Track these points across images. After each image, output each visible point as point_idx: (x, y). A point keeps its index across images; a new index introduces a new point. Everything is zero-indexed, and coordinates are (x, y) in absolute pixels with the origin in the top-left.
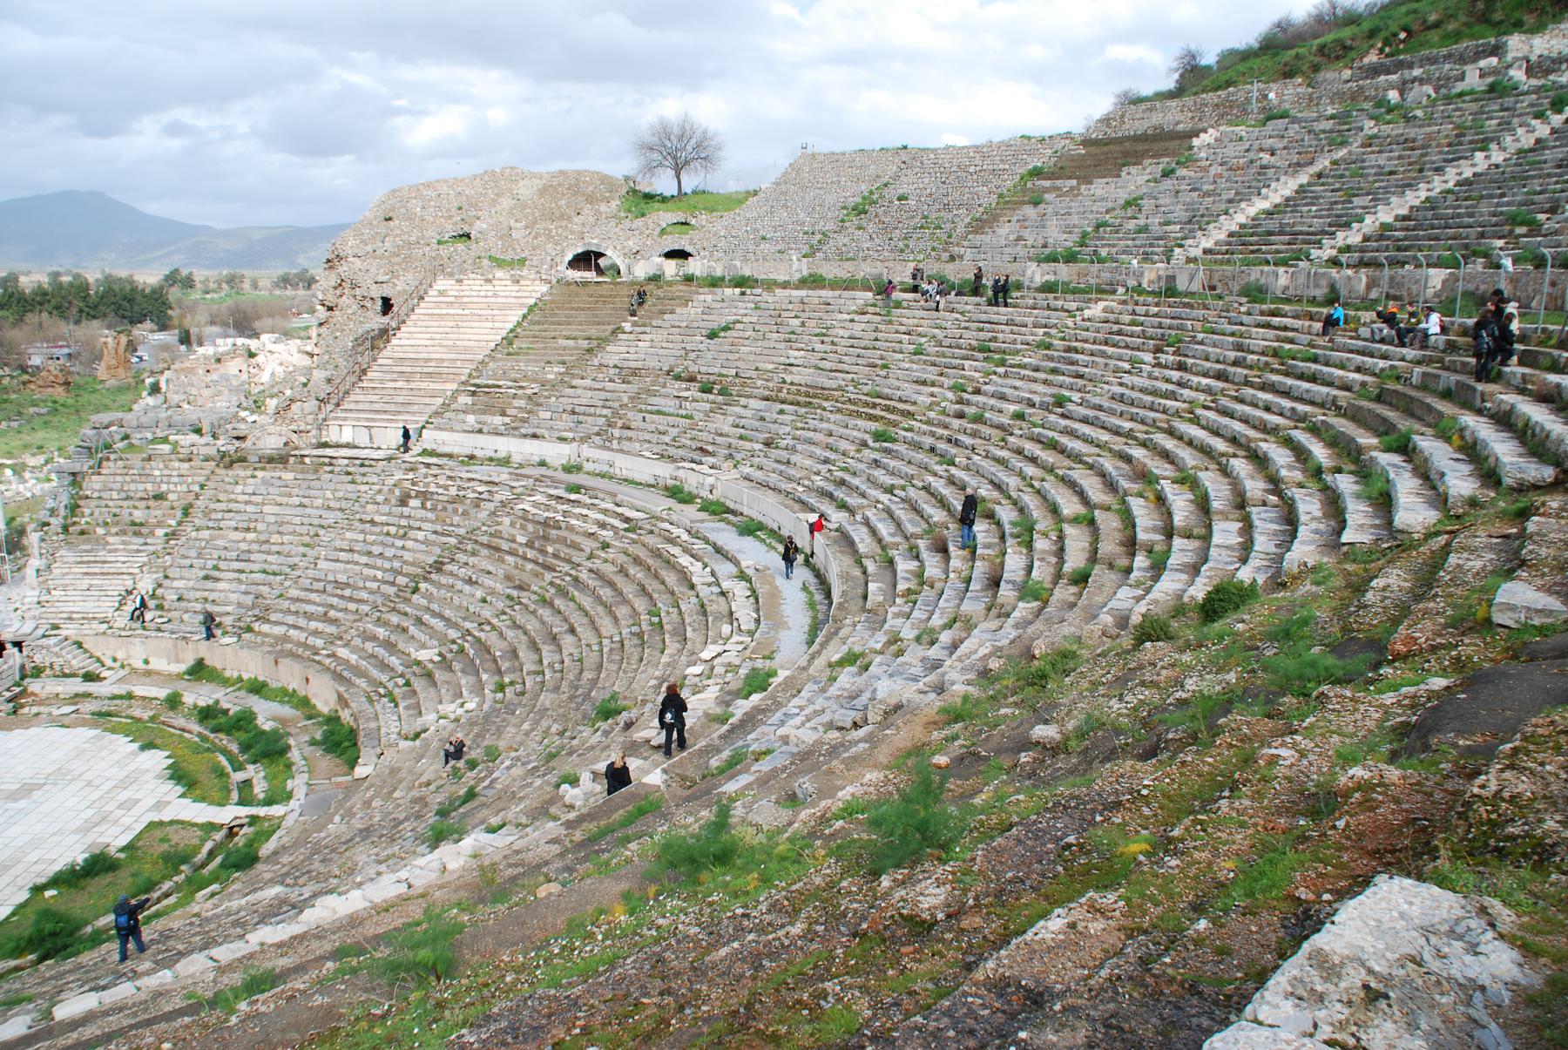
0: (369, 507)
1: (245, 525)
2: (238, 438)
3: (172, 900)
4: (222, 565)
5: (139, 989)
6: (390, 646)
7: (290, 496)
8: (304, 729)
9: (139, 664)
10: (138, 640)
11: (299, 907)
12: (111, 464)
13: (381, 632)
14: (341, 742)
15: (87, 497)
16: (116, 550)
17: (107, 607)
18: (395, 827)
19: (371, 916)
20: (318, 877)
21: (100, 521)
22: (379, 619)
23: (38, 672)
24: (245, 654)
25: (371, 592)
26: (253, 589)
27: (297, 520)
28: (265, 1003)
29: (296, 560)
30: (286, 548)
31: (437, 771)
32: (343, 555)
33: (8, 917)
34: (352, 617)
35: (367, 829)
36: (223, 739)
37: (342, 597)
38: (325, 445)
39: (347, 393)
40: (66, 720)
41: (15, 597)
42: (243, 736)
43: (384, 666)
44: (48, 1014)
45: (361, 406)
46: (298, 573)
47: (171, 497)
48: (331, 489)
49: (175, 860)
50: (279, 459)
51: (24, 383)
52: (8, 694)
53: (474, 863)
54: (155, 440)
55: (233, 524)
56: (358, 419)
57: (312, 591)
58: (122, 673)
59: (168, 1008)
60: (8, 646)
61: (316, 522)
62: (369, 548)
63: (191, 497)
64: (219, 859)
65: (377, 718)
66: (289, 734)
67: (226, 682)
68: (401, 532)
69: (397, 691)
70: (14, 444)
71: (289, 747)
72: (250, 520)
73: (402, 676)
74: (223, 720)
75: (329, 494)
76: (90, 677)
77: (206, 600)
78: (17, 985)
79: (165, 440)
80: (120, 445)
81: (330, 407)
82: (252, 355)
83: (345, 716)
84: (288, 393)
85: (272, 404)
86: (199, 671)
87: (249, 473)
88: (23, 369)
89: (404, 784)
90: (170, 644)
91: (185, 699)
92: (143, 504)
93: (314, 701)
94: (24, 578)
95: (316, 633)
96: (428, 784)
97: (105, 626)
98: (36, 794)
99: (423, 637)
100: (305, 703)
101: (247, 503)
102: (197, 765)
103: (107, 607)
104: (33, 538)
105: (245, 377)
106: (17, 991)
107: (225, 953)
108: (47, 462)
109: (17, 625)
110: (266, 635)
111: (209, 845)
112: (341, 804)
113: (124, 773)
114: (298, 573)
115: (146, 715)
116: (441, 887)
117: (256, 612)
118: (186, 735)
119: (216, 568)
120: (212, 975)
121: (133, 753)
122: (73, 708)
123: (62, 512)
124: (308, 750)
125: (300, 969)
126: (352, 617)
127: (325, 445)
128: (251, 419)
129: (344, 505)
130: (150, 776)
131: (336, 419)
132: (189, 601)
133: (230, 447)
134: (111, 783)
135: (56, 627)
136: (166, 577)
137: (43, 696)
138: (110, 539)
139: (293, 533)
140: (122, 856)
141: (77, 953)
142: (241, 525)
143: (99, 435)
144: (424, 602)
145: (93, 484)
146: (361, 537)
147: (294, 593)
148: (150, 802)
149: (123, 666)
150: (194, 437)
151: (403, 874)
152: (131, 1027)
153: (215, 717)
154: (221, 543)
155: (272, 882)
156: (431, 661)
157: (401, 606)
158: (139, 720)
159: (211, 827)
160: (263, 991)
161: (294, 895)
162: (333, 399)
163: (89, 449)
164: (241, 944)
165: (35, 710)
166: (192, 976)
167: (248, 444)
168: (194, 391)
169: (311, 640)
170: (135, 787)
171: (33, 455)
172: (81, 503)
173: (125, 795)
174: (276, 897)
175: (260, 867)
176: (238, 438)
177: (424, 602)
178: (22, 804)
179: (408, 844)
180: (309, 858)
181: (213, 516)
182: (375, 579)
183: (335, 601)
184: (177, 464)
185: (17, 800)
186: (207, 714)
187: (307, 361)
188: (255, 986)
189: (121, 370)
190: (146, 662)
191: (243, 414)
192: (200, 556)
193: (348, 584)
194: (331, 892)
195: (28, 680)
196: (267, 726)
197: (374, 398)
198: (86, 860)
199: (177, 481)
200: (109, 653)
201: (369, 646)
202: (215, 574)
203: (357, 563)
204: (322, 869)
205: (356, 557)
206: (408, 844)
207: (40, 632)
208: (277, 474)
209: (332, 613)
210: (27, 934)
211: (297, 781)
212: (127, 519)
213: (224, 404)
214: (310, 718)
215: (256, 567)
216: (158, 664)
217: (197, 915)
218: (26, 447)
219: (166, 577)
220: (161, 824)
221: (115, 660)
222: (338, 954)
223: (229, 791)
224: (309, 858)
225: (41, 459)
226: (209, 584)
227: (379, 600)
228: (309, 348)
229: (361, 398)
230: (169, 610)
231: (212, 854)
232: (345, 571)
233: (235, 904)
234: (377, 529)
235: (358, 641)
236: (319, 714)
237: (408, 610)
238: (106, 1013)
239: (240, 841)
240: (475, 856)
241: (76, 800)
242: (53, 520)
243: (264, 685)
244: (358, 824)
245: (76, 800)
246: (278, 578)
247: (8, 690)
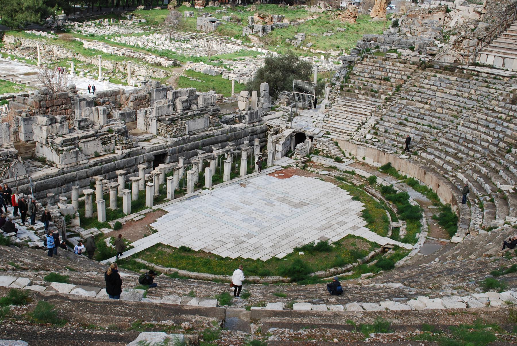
0: (494, 102)
1: (425, 100)
2: (431, 55)
3: (350, 273)
4: (410, 119)
5: (328, 309)
6: (487, 179)
7: (452, 89)
8: (431, 210)
9: (360, 159)
10: (362, 147)
11: (409, 297)
12: (368, 60)
13: (484, 170)
14: (448, 222)
15: (354, 74)
16: (362, 102)
17: (351, 128)
18: (467, 273)
19: (444, 314)
20: (421, 286)
21: (357, 86)
22: (484, 163)
23: (317, 152)
24: (411, 165)
25: (484, 147)
26: (422, 133)
27: (453, 102)
28: (383, 337)
29: (447, 123)
30: (443, 116)
31: (497, 251)
32: (472, 125)
33: (284, 258)
34: (469, 159)
35: (451, 270)
36: (391, 205)
37: (467, 147)
38: (477, 65)
39: (496, 37)
40: (324, 177)
41: (314, 116)
42: (401, 206)
43: (481, 188)
44: (291, 306)
45: (502, 45)
46: (446, 130)
47: (392, 80)
48: (474, 89)
49: (356, 255)
50: (450, 69)
51: (337, 15)
52: (303, 159)
53: (507, 307)
54: (391, 51)
55: (419, 99)
56: (499, 52)
57: (452, 141)
58: (352, 161)
59: (339, 323)
60: (307, 138)
61: (462, 105)
62: (488, 124)
63: (401, 82)
64: (375, 261)
65: (470, 214)
66: (423, 210)
67: (398, 177)
68: (508, 118)
69: (485, 202)
70: (327, 44)
71: (421, 217)
72: (428, 99)
73: (490, 195)
74: (392, 195)
75: (472, 91)
76: (338, 160)
77: (398, 134)
78: (281, 289)
79: (395, 51)
80: (374, 51)
81: (484, 44)
82: (448, 11)
83: (454, 208)
84: (463, 33)
85: (453, 38)
86: (387, 169)
87: (433, 74)
88: (338, 8)
89: (477, 252)
90: (376, 152)
91: (377, 181)
92: (379, 81)
93: (439, 197)
94: (319, 108)
95: (449, 163)
96: (490, 256)
97: (349, 137)
98: (305, 207)
99: (506, 177)
100: (434, 197)
101: (429, 89)
102: (375, 213)
103: (351, 128)
104: (327, 90)
105: (442, 22)
106: (281, 291)
107: (370, 307)
108: (339, 55)
109: (313, 129)
110: (423, 158)
111: (372, 253)
112: (441, 253)
113: (342, 208)
114: (446, 130)
115: (358, 184)
116: (485, 313)
117: (421, 145)
118: (374, 198)
119: (406, 119)
120: (361, 315)
121: (348, 200)
122: (328, 172)
123: (342, 80)
124: (431, 221)
125: (402, 328)
126: (469, 159)
127: (477, 65)
128: (440, 46)
129: (479, 98)
130: (354, 213)
131: (486, 51)
132: (390, 133)
133: (426, 59)
134: (337, 212)
135: (328, 133)
136: (382, 120)
137: (317, 164)
138: (360, 96)
139: (449, 109)
140: (334, 246)
141: (306, 284)
142: (423, 100)
143: (365, 44)
144: (512, 159)
145: (358, 68)
146: (485, 117)
147: (442, 140)
148: (351, 225)
149: (353, 158)
150: (409, 52)
151: (466, 299)
152: (322, 325)
153: (390, 193)
154: (411, 107)
155: (398, 280)
156: (508, 192)
157: (498, 158)
158: (354, 185)
159: (375, 245)
160: (383, 332)
161: (407, 290)
162: (487, 39)
163: (359, 51)
164: (377, 305)
165: (312, 169)
166: (353, 312)
167: (436, 58)
168: (414, 27)
169: (445, 166)
170: (346, 216)
171: (334, 50)
172: (351, 76)
173: (341, 219)
174: (398, 288)
175: (394, 271)
176: (431, 55)
177: (512, 159)
178: (299, 210)
179: (471, 284)
180: (419, 275)
181: (411, 93)
182: (487, 141)
183: (463, 148)
184: (398, 64)
185: (297, 208)
186: (386, 190)
187: (477, 17)
188: (381, 327)
189: (381, 13)
190: (364, 158)
191: (436, 42)
192: (399, 112)
193: (471, 141)
194: (426, 295)
195: (312, 155)
196: (413, 204)
197: (511, 41)
198: (318, 243)
199: (396, 72)
200: (349, 151)
201: (475, 176)
202: (405, 122)
203: (479, 131)
204: (423, 282)
205: (480, 127)
206: (471, 284)
207: (321, 134)
208: (448, 77)
209: (460, 154)
210: (289, 268)
211: (421, 235)
212: (369, 87)
213: (428, 36)
214: (435, 205)
215: (426, 123)
216: (369, 161)
217: (360, 284)
218: (332, 46)
219: (382, 120)
220: (354, 236)
221: (350, 154)
222: (421, 327)
223: (388, 230)
224: (419, 275)
225: (337, 53)
226: (401, 127)
227: (487, 153)
228: (480, 10)
229: (503, 40)
230: (380, 136)
231: (373, 258)
232: (472, 134)
233: (378, 285)
234: (495, 115)
235: (470, 172)
236: (441, 204)
237: (502, 161)
238: (314, 315)
239: (387, 255)
240: (508, 303)
241: (320, 215)
242: (337, 83)
243: (416, 183)
244: (447, 265)
245: (320, 215)
246: (436, 131)
247: (303, 158)
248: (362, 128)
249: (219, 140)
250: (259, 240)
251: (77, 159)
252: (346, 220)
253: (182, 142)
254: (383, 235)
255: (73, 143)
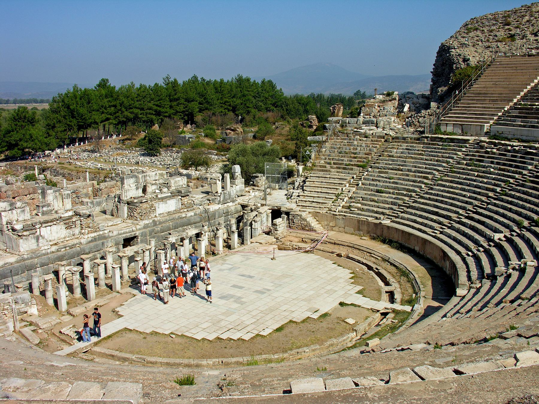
241: (306, 285)
245: (306, 285)
248: (339, 200)
249: (192, 221)
250: (239, 317)
251: (38, 245)
252: (336, 289)
253: (153, 224)
254: (379, 300)
255: (34, 228)
